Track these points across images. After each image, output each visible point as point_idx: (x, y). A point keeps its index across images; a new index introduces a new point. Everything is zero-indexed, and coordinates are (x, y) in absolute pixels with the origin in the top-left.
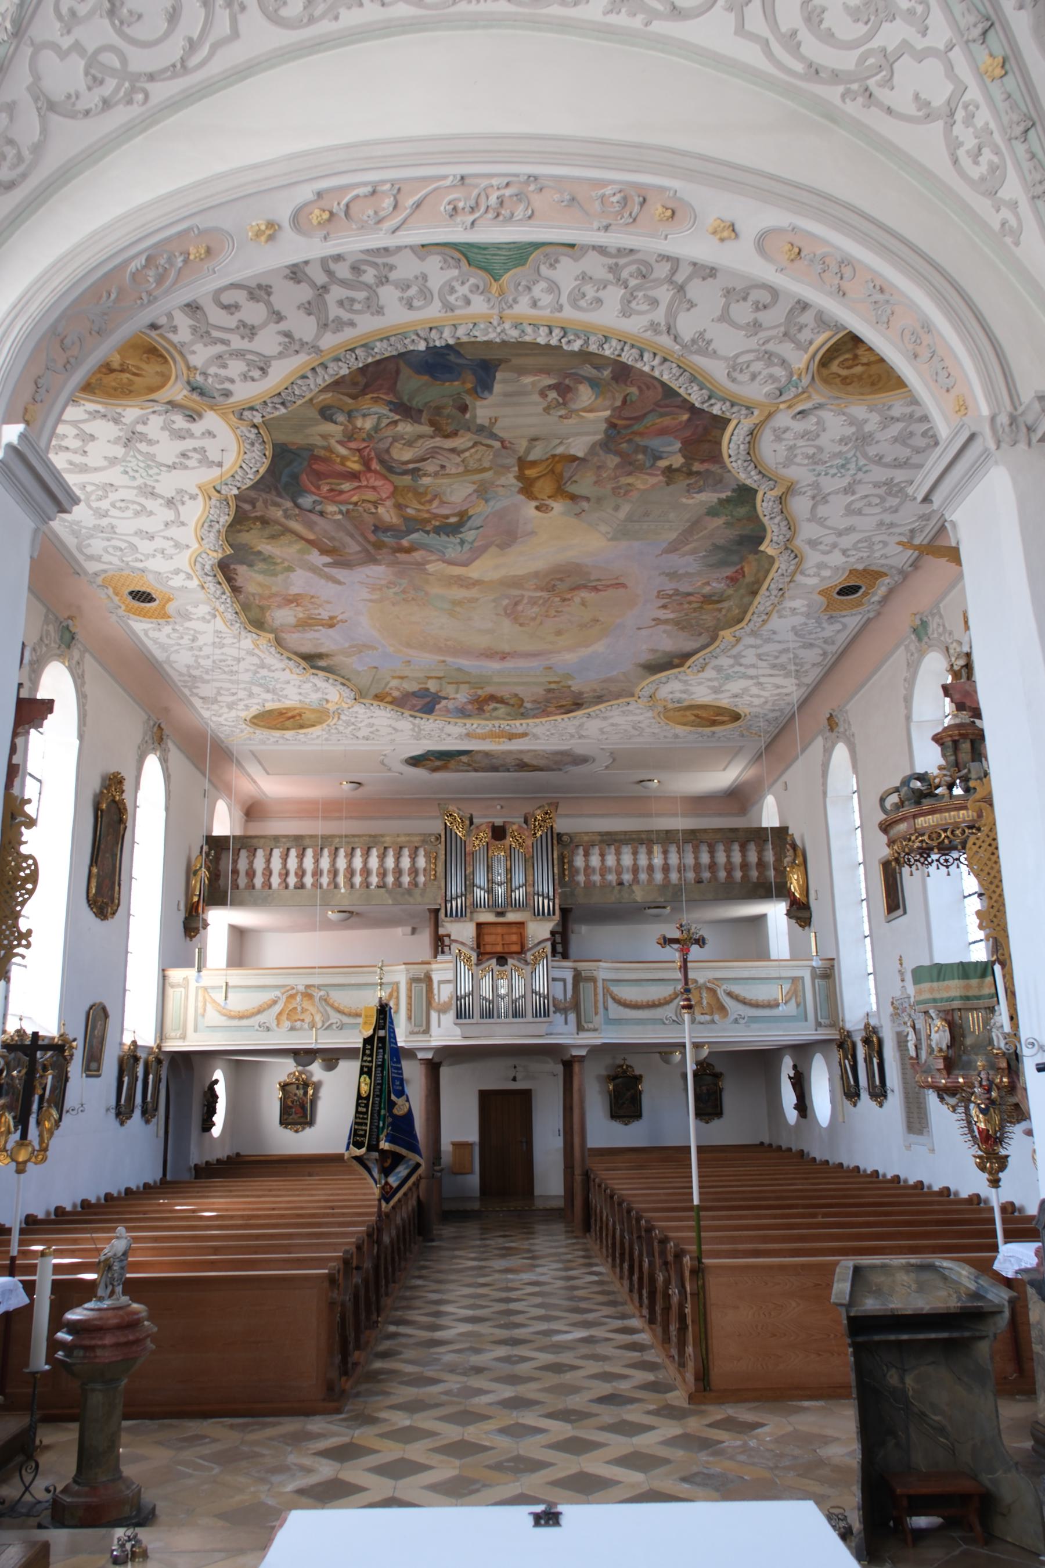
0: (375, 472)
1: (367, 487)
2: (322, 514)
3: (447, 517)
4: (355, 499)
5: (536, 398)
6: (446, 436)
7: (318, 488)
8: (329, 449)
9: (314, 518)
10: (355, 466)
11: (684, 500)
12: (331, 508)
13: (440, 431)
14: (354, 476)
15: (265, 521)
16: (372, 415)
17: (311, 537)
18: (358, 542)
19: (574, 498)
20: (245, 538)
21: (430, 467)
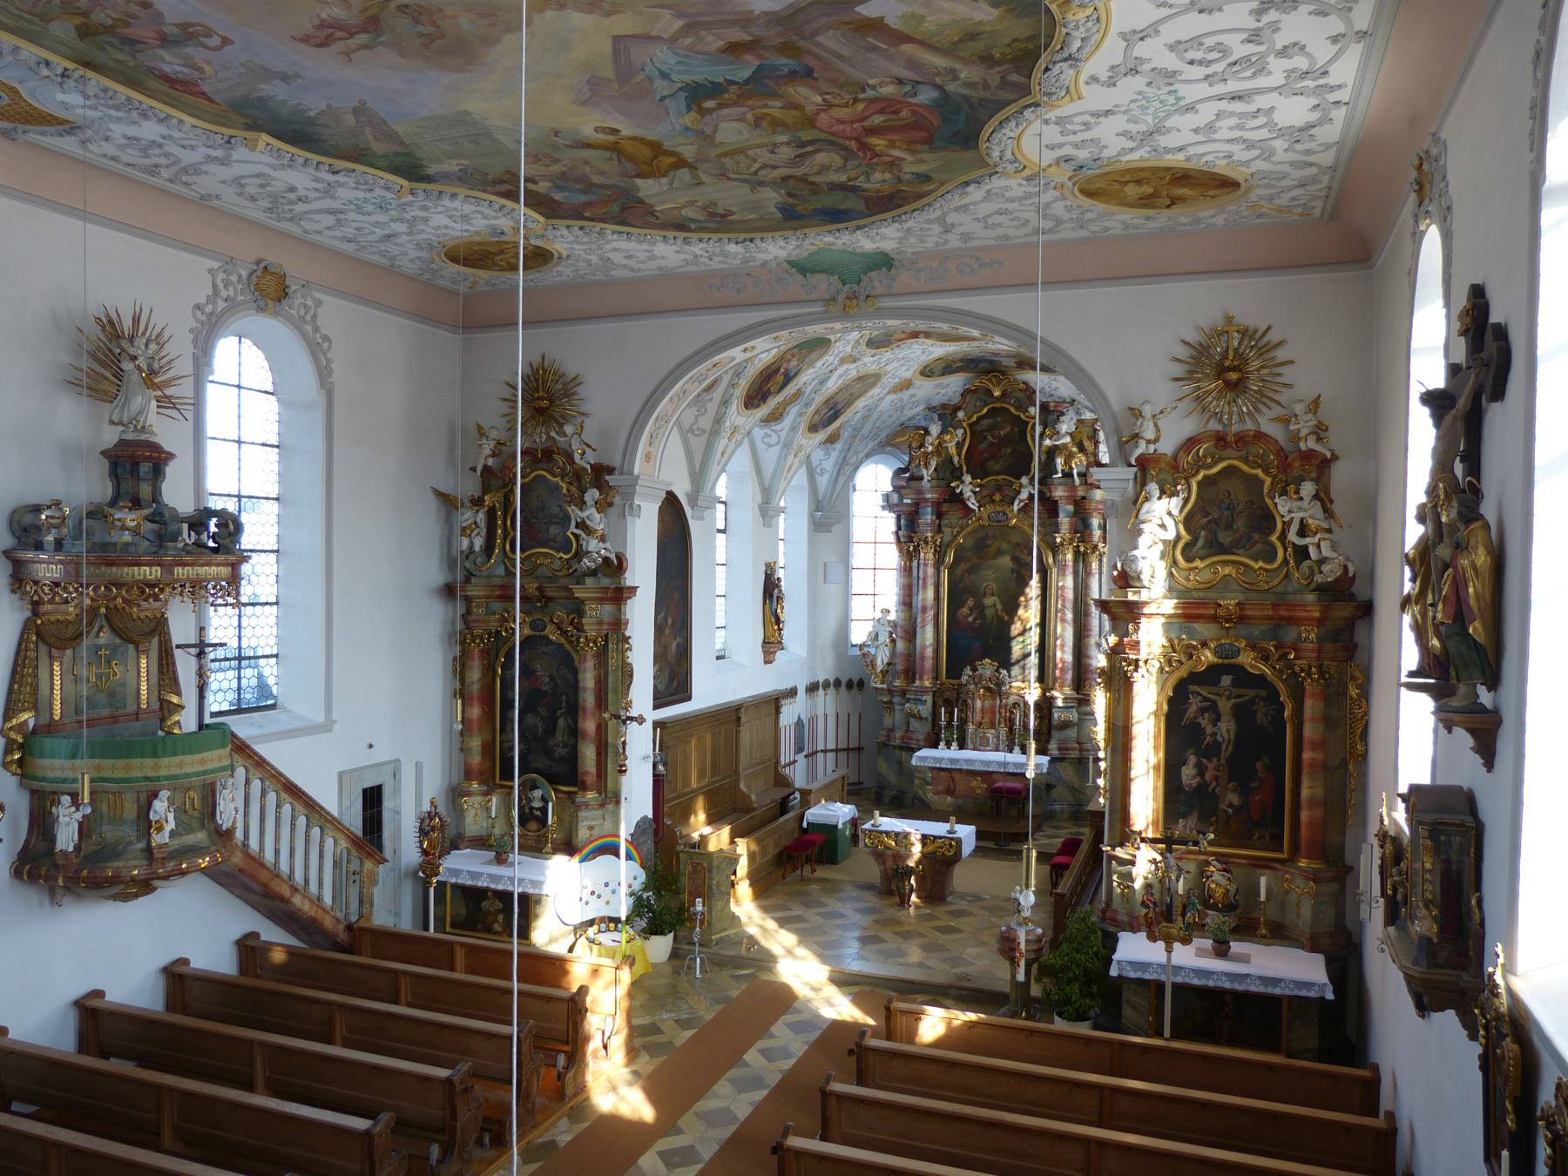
0: (850, 139)
1: (852, 122)
2: (900, 82)
3: (721, 106)
4: (860, 107)
5: (734, 209)
6: (790, 177)
7: (914, 113)
8: (913, 152)
9: (905, 74)
10: (876, 142)
11: (465, 162)
12: (889, 90)
13: (803, 179)
14: (872, 131)
15: (987, 60)
16: (878, 180)
17: (908, 48)
18: (827, 50)
19: (588, 146)
20: (1020, 29)
21: (786, 152)
